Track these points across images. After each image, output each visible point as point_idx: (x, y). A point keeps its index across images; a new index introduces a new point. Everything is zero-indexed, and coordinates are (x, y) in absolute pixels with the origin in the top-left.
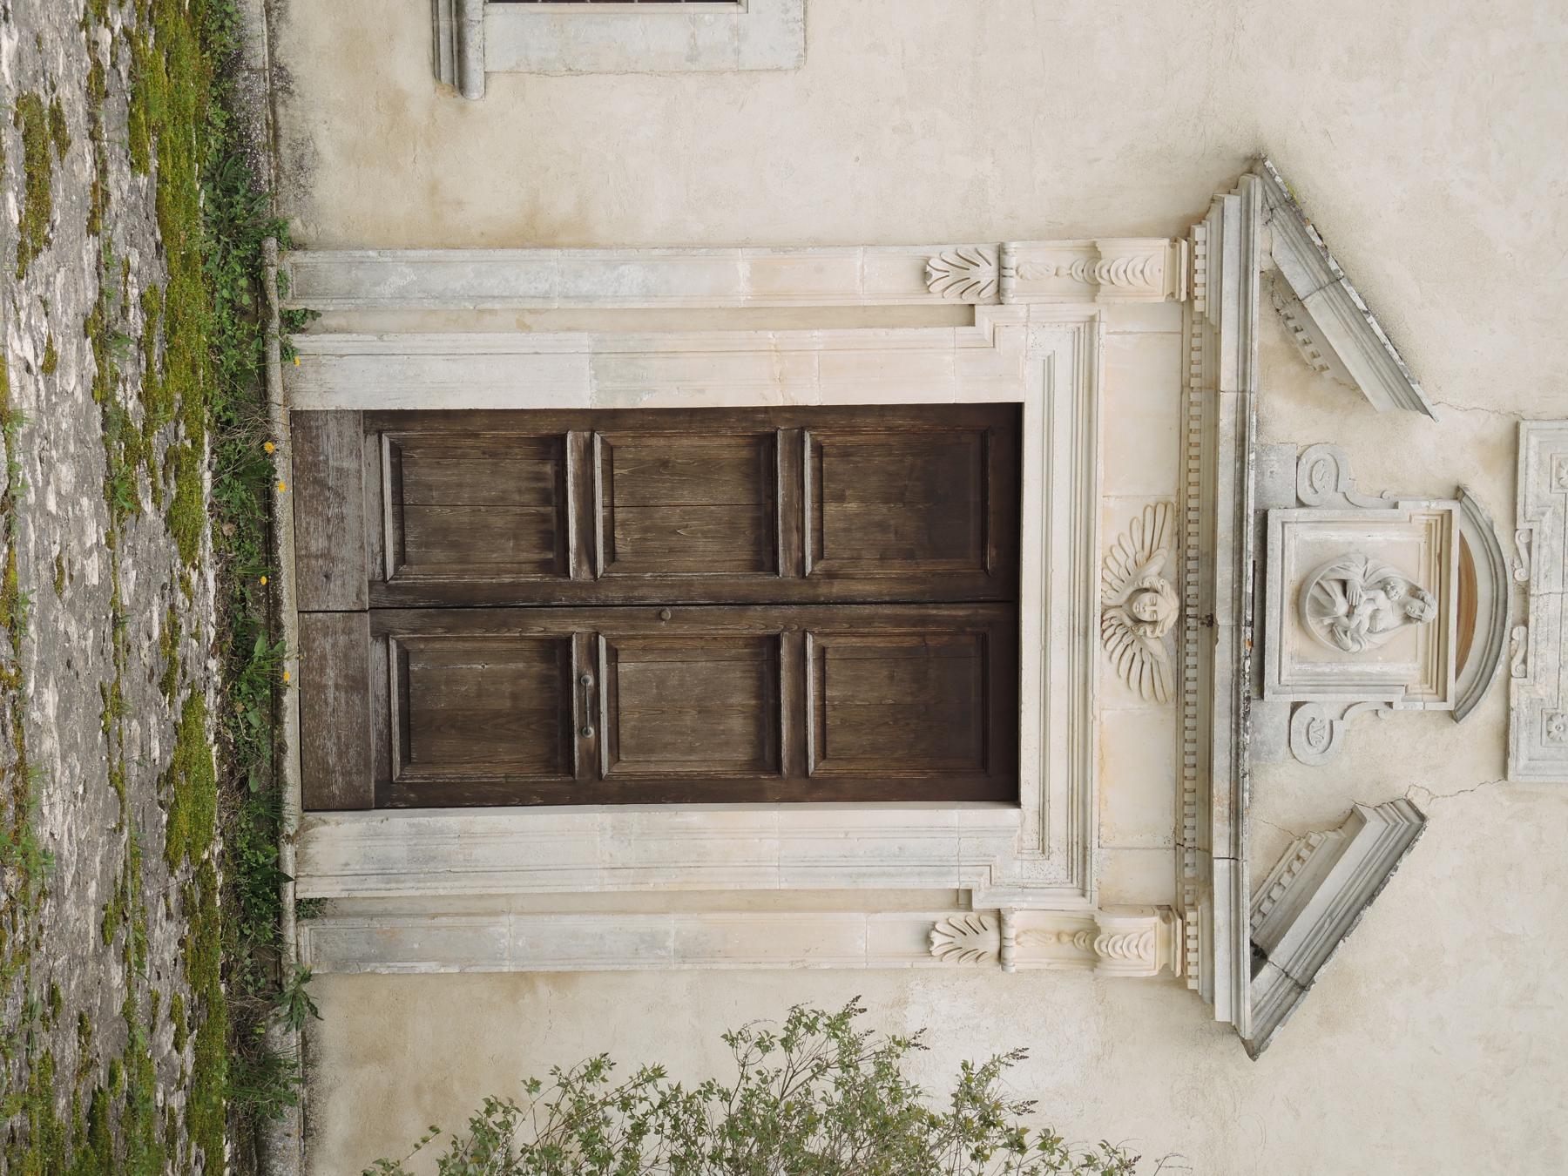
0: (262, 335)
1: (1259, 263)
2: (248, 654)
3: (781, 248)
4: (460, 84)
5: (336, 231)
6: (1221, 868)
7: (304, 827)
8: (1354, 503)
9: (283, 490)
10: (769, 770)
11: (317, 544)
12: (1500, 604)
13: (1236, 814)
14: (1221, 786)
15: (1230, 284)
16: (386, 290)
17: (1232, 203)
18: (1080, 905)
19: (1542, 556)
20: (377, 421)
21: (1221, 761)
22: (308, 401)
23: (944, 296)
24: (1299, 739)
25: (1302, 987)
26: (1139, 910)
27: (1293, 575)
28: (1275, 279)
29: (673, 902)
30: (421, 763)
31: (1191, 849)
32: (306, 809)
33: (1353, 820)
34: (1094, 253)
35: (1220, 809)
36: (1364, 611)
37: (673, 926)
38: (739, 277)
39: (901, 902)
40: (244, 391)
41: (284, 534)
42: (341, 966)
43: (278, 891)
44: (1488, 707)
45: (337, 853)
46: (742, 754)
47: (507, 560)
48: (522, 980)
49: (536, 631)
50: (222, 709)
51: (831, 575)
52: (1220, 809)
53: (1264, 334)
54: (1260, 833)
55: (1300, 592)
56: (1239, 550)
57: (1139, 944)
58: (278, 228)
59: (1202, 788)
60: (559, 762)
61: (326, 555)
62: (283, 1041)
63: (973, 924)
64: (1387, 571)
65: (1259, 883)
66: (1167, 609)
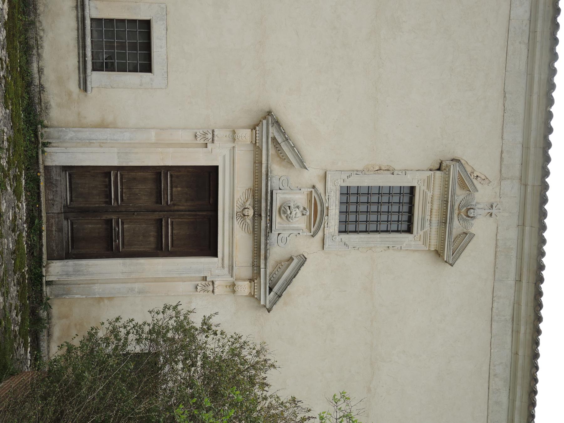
0: (37, 148)
1: (271, 135)
2: (34, 223)
3: (162, 129)
4: (85, 90)
5: (55, 123)
6: (262, 270)
7: (48, 264)
8: (292, 188)
9: (42, 184)
10: (159, 250)
11: (51, 197)
12: (322, 211)
13: (266, 258)
14: (262, 252)
15: (264, 140)
16: (67, 137)
17: (265, 122)
18: (231, 279)
19: (331, 201)
20: (65, 168)
21: (263, 247)
22: (49, 163)
23: (200, 141)
24: (280, 241)
25: (280, 296)
26: (244, 280)
27: (278, 205)
28: (274, 139)
29: (137, 280)
31: (256, 266)
32: (48, 260)
33: (291, 259)
34: (234, 132)
36: (294, 213)
37: (137, 286)
38: (152, 136)
39: (190, 280)
40: (32, 161)
41: (43, 195)
42: (57, 296)
43: (41, 279)
44: (320, 234)
45: (56, 270)
46: (153, 246)
47: (97, 201)
48: (101, 299)
49: (104, 218)
50: (27, 236)
51: (174, 205)
52: (262, 257)
53: (272, 151)
54: (271, 262)
55: (280, 209)
56: (267, 199)
57: (244, 288)
58: (41, 123)
59: (258, 253)
61: (53, 200)
62: (43, 314)
63: (207, 284)
64: (299, 204)
65: (270, 274)
66: (251, 212)
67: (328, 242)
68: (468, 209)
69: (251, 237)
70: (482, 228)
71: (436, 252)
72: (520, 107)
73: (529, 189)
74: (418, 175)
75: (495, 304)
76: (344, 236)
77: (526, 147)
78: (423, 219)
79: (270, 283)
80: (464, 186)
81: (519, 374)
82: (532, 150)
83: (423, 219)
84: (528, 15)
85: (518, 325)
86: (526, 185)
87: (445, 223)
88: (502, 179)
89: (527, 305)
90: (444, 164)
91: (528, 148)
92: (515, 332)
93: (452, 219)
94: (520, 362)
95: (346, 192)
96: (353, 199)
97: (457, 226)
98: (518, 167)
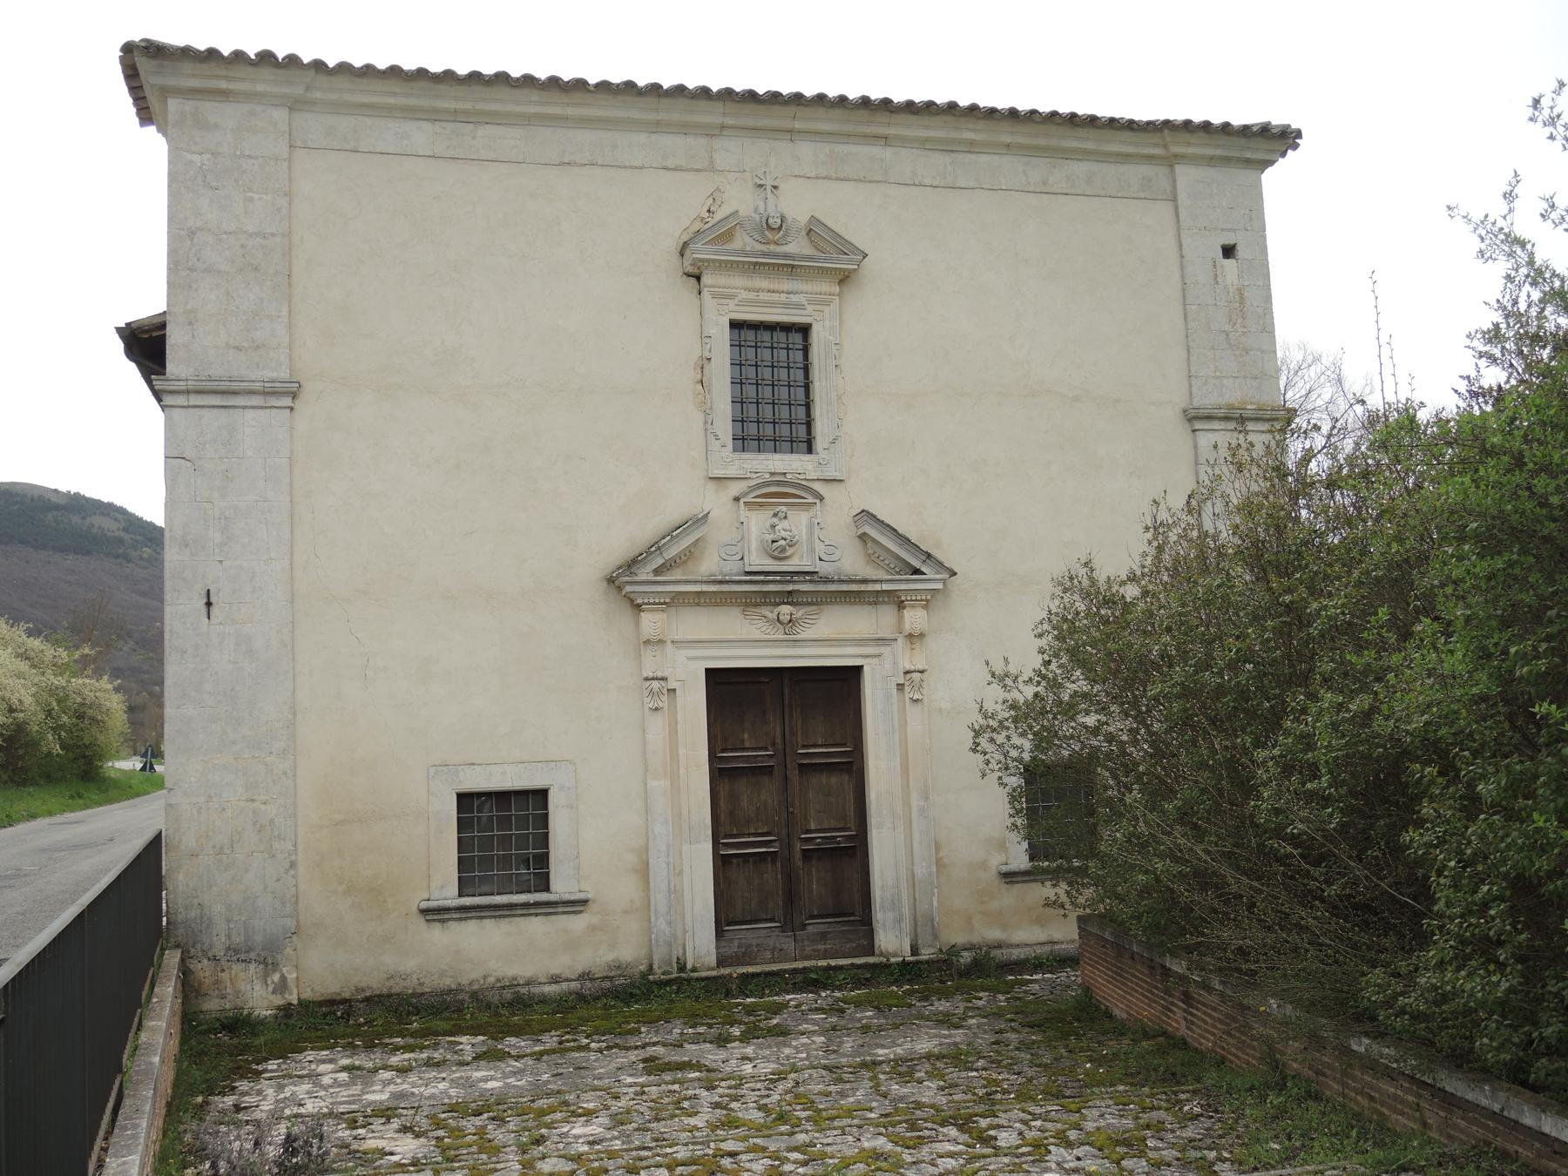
0: (689, 980)
1: (651, 577)
2: (816, 980)
3: (646, 770)
4: (585, 902)
5: (644, 951)
6: (885, 587)
7: (881, 954)
8: (739, 539)
9: (751, 969)
10: (853, 766)
11: (768, 955)
12: (778, 483)
13: (865, 581)
14: (854, 587)
15: (660, 588)
16: (667, 930)
17: (629, 588)
18: (901, 641)
19: (759, 468)
20: (720, 933)
21: (845, 587)
22: (713, 960)
23: (664, 702)
24: (833, 558)
25: (929, 556)
26: (901, 619)
27: (770, 561)
28: (657, 572)
29: (907, 804)
30: (853, 907)
31: (876, 599)
32: (873, 954)
33: (863, 537)
34: (647, 642)
35: (863, 587)
36: (784, 534)
37: (916, 803)
38: (658, 785)
39: (903, 711)
40: (715, 988)
41: (767, 968)
42: (936, 937)
43: (909, 963)
44: (817, 486)
45: (891, 940)
46: (846, 778)
47: (772, 877)
48: (939, 863)
49: (800, 864)
50: (840, 990)
51: (774, 744)
52: (863, 587)
53: (677, 575)
55: (776, 558)
56: (763, 582)
57: (914, 618)
58: (644, 976)
59: (854, 595)
60: (851, 852)
61: (773, 951)
62: (966, 957)
63: (909, 683)
65: (889, 573)
70: (799, 203)
71: (841, 282)
72: (587, 137)
73: (729, 121)
74: (710, 314)
75: (927, 181)
76: (819, 444)
77: (657, 127)
78: (786, 305)
79: (903, 573)
80: (728, 236)
82: (662, 116)
83: (786, 305)
84: (427, 126)
85: (960, 142)
86: (723, 127)
87: (793, 267)
88: (711, 168)
89: (927, 127)
90: (690, 269)
91: (658, 123)
92: (972, 147)
93: (786, 256)
95: (743, 442)
96: (752, 429)
97: (797, 246)
98: (690, 140)
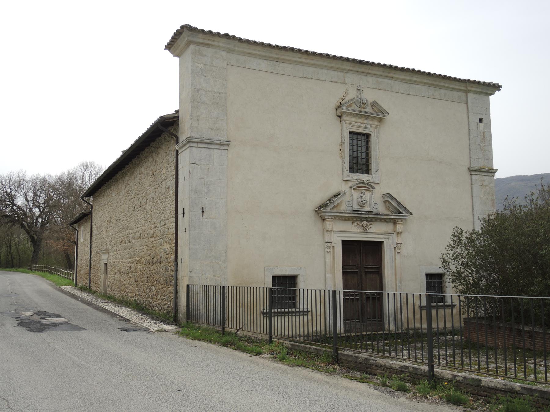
3: (325, 271)
6: (391, 217)
8: (351, 201)
10: (379, 272)
14: (385, 217)
15: (332, 214)
18: (395, 235)
19: (357, 178)
25: (405, 208)
26: (395, 227)
27: (359, 207)
28: (331, 209)
30: (378, 317)
34: (327, 231)
35: (387, 217)
51: (358, 264)
54: (386, 212)
57: (399, 227)
64: (359, 196)
66: (365, 222)
67: (376, 181)
68: (363, 103)
69: (375, 223)
70: (370, 96)
71: (380, 122)
72: (311, 69)
73: (352, 69)
74: (345, 129)
75: (402, 92)
77: (330, 68)
78: (365, 128)
79: (396, 212)
80: (350, 105)
81: (434, 83)
82: (333, 65)
83: (365, 128)
84: (265, 61)
85: (411, 81)
86: (349, 70)
87: (368, 116)
88: (344, 83)
89: (404, 75)
90: (339, 114)
91: (331, 67)
92: (415, 82)
93: (365, 112)
94: (429, 82)
95: (352, 170)
96: (355, 166)
97: (369, 109)
98: (339, 73)
